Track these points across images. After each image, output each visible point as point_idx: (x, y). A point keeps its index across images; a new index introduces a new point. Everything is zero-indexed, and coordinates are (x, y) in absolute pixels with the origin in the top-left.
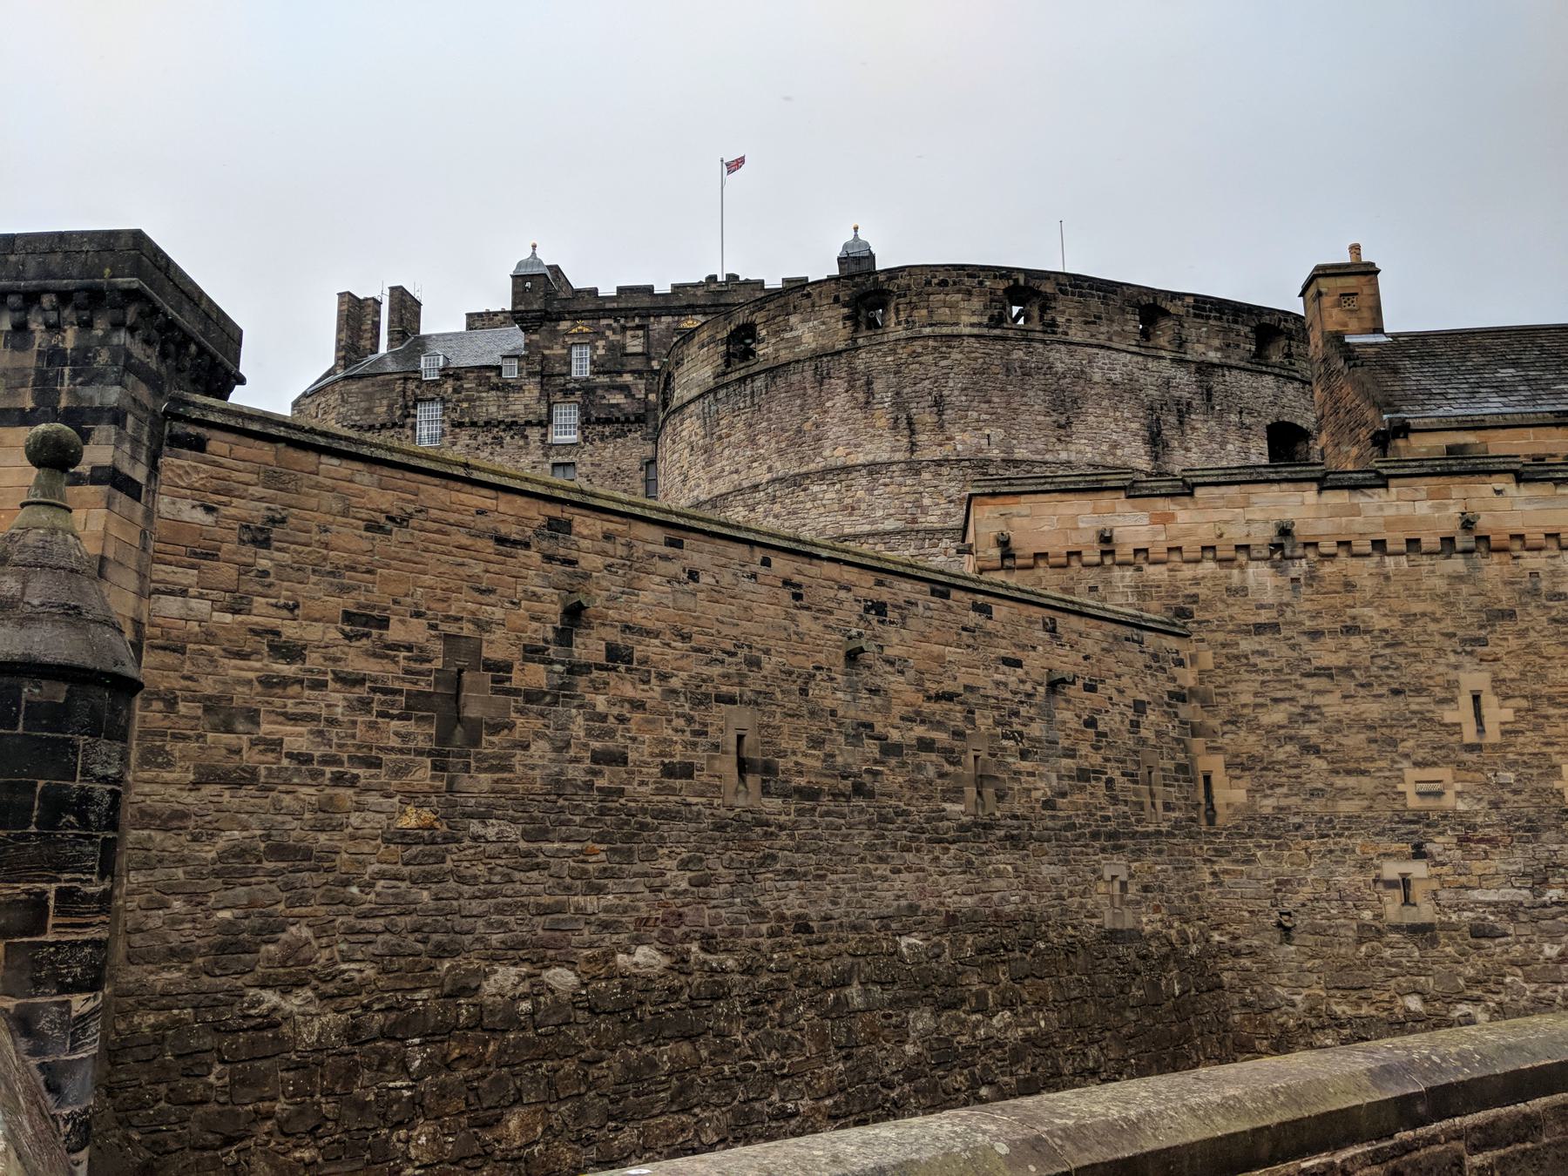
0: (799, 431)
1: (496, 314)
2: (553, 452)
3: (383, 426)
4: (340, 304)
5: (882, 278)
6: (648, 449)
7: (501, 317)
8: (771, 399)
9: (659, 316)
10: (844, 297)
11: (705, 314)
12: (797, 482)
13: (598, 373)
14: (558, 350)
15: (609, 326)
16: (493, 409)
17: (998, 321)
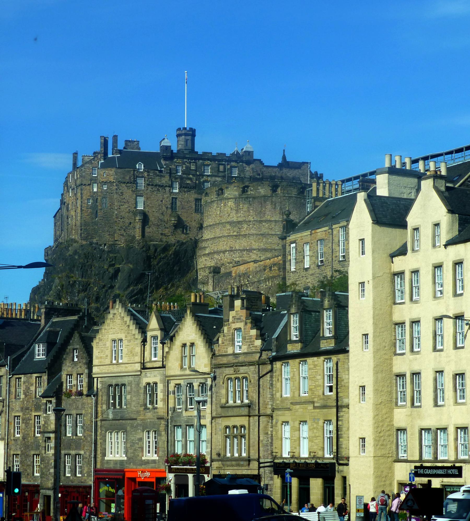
0: (260, 211)
1: (134, 141)
2: (172, 194)
3: (128, 183)
4: (101, 140)
5: (278, 183)
6: (196, 196)
7: (136, 143)
8: (254, 203)
9: (199, 160)
10: (271, 185)
11: (211, 161)
12: (261, 222)
13: (184, 174)
14: (173, 167)
15: (186, 161)
16: (158, 182)
17: (298, 194)
